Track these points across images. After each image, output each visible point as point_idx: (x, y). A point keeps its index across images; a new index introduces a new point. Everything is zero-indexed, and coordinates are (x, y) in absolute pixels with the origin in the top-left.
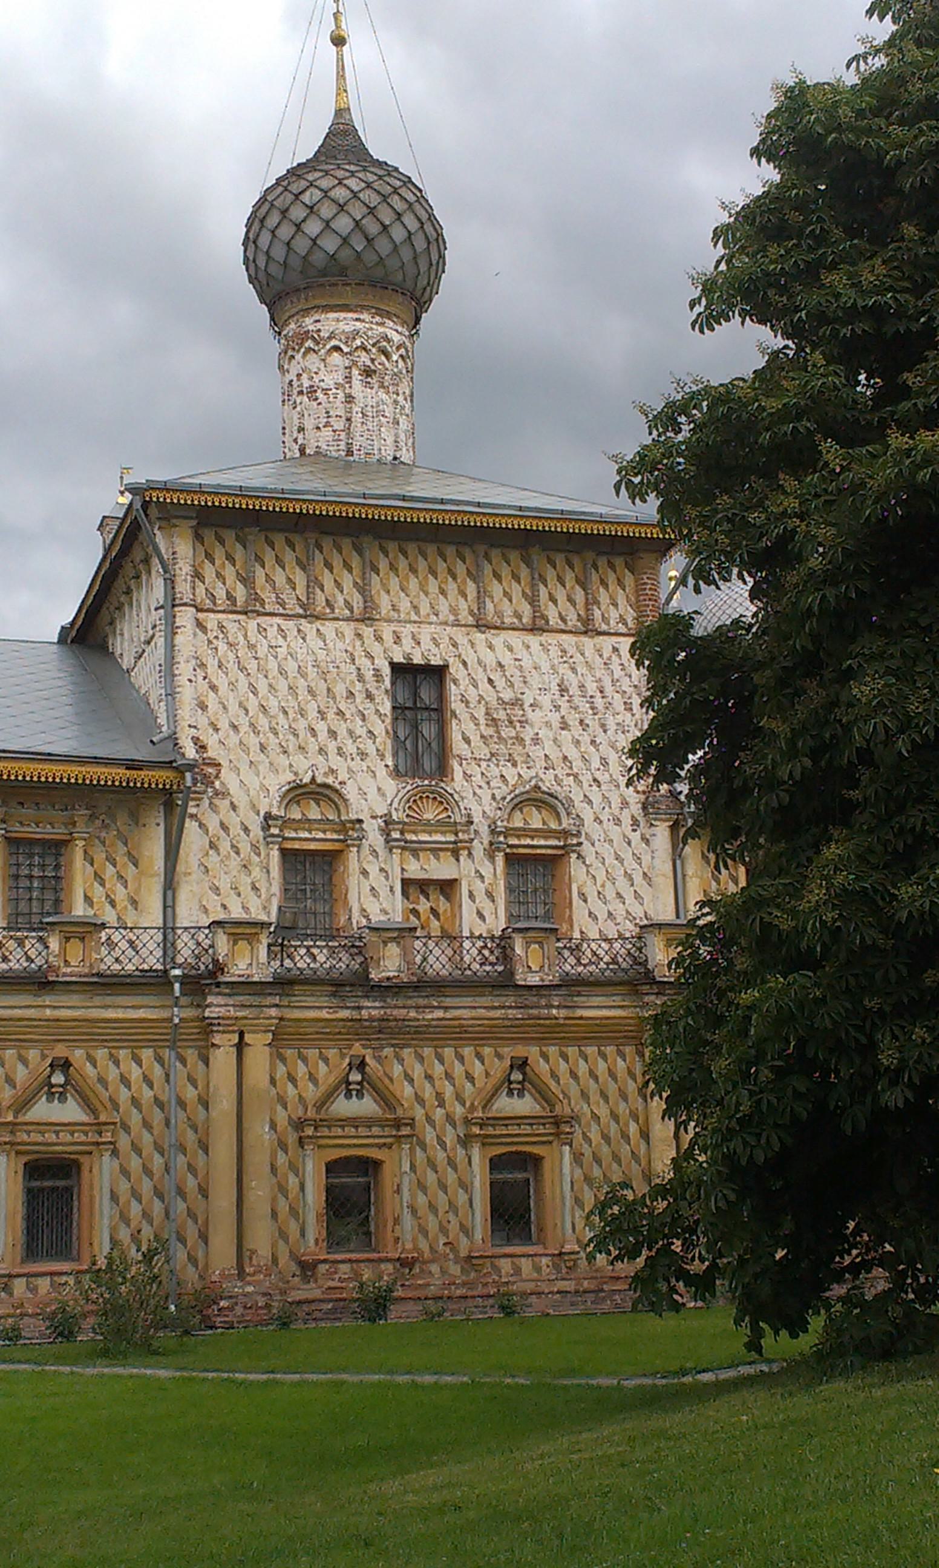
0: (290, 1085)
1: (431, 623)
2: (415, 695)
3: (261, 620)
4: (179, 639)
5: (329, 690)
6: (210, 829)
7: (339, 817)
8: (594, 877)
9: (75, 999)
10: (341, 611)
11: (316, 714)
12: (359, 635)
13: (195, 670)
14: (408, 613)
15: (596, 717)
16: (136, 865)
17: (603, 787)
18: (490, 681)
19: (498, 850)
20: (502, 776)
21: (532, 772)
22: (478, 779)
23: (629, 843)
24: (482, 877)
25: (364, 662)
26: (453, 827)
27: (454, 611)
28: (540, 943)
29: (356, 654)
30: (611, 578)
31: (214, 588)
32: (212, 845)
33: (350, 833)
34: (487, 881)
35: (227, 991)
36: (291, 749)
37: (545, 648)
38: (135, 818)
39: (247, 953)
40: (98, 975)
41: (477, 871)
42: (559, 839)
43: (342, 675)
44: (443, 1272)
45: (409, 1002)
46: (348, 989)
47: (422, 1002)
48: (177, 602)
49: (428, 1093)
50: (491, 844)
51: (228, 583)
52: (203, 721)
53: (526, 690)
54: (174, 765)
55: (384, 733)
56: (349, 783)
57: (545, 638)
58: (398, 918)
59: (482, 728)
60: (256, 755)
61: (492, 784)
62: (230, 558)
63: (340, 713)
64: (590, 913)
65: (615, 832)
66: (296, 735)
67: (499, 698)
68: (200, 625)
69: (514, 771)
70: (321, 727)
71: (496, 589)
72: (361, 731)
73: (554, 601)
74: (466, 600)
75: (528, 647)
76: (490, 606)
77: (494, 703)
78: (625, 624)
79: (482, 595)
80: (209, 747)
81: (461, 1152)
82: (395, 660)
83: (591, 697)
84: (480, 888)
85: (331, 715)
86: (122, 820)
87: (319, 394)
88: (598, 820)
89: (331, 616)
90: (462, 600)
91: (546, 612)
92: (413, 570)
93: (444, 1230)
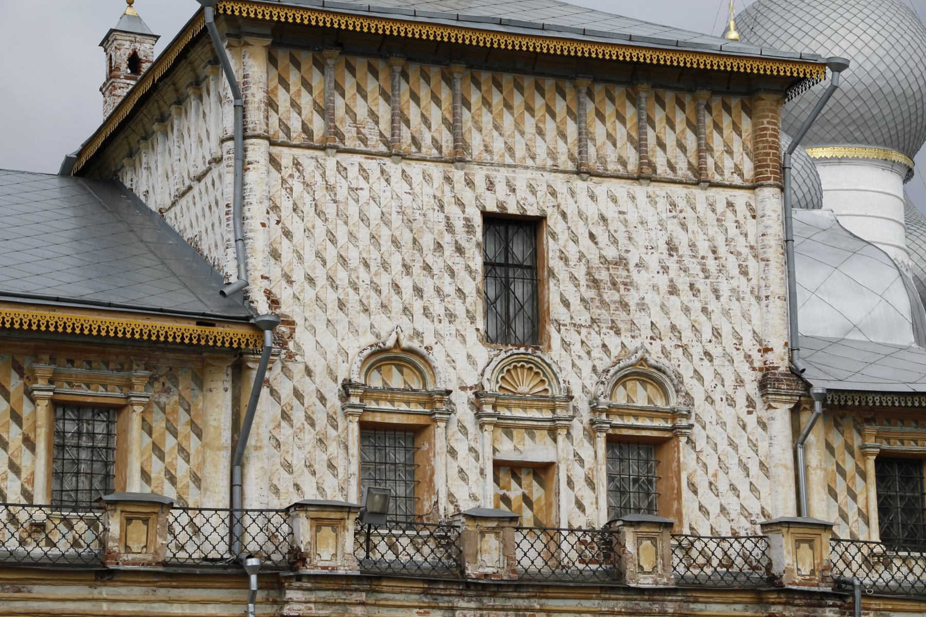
1: (527, 168)
2: (507, 250)
3: (341, 157)
4: (251, 177)
5: (415, 241)
6: (283, 397)
7: (424, 385)
8: (705, 465)
9: (136, 591)
10: (428, 150)
13: (268, 213)
14: (502, 156)
15: (708, 281)
16: (199, 436)
17: (716, 362)
18: (592, 236)
19: (600, 430)
20: (604, 346)
21: (637, 343)
22: (577, 348)
23: (744, 427)
24: (581, 461)
25: (453, 211)
26: (551, 403)
27: (552, 154)
28: (653, 540)
29: (445, 200)
30: (726, 121)
31: (289, 119)
32: (285, 416)
33: (438, 405)
34: (587, 466)
35: (309, 585)
38: (199, 381)
39: (331, 541)
40: (165, 564)
41: (576, 454)
42: (666, 419)
43: (430, 225)
45: (510, 603)
46: (441, 586)
47: (521, 603)
48: (249, 133)
50: (592, 422)
51: (304, 112)
52: (275, 272)
53: (631, 248)
54: (252, 321)
55: (474, 291)
56: (436, 348)
57: (654, 188)
58: (488, 504)
59: (583, 289)
60: (334, 313)
61: (593, 354)
63: (427, 268)
64: (701, 507)
65: (729, 415)
66: (378, 291)
67: (601, 257)
68: (274, 161)
70: (406, 284)
71: (599, 130)
72: (449, 289)
73: (662, 145)
74: (566, 142)
75: (633, 198)
76: (592, 150)
77: (595, 262)
78: (741, 175)
79: (584, 137)
80: (282, 301)
83: (703, 258)
84: (579, 474)
85: (417, 269)
86: (185, 382)
88: (709, 399)
89: (418, 155)
90: (561, 142)
91: (653, 160)
92: (508, 106)
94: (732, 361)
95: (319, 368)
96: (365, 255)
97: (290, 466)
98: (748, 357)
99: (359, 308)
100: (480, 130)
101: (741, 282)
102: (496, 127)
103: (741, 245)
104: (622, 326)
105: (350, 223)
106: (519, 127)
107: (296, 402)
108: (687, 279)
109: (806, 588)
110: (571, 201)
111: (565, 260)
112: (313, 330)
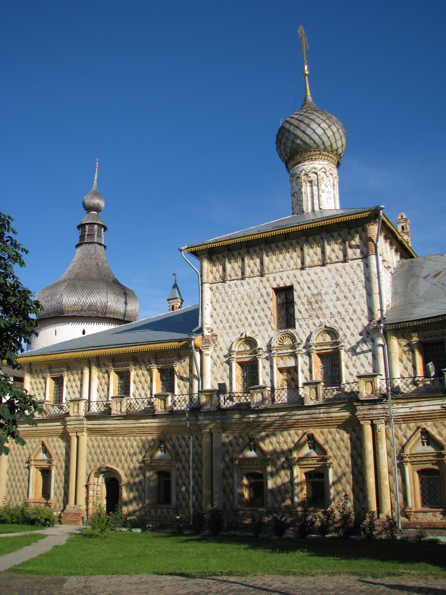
0: (230, 447)
5: (251, 303)
11: (247, 312)
17: (354, 321)
18: (309, 288)
20: (314, 323)
22: (304, 326)
36: (239, 327)
37: (330, 270)
43: (256, 296)
53: (322, 288)
60: (229, 330)
63: (256, 310)
66: (241, 321)
67: (312, 294)
68: (211, 289)
69: (318, 321)
70: (249, 317)
72: (262, 315)
77: (310, 296)
82: (274, 287)
83: (349, 286)
85: (252, 311)
87: (295, 195)
94: (360, 320)
96: (237, 311)
97: (216, 378)
99: (235, 327)
102: (277, 260)
104: (320, 316)
105: (232, 301)
107: (218, 359)
109: (368, 399)
110: (301, 278)
111: (299, 297)
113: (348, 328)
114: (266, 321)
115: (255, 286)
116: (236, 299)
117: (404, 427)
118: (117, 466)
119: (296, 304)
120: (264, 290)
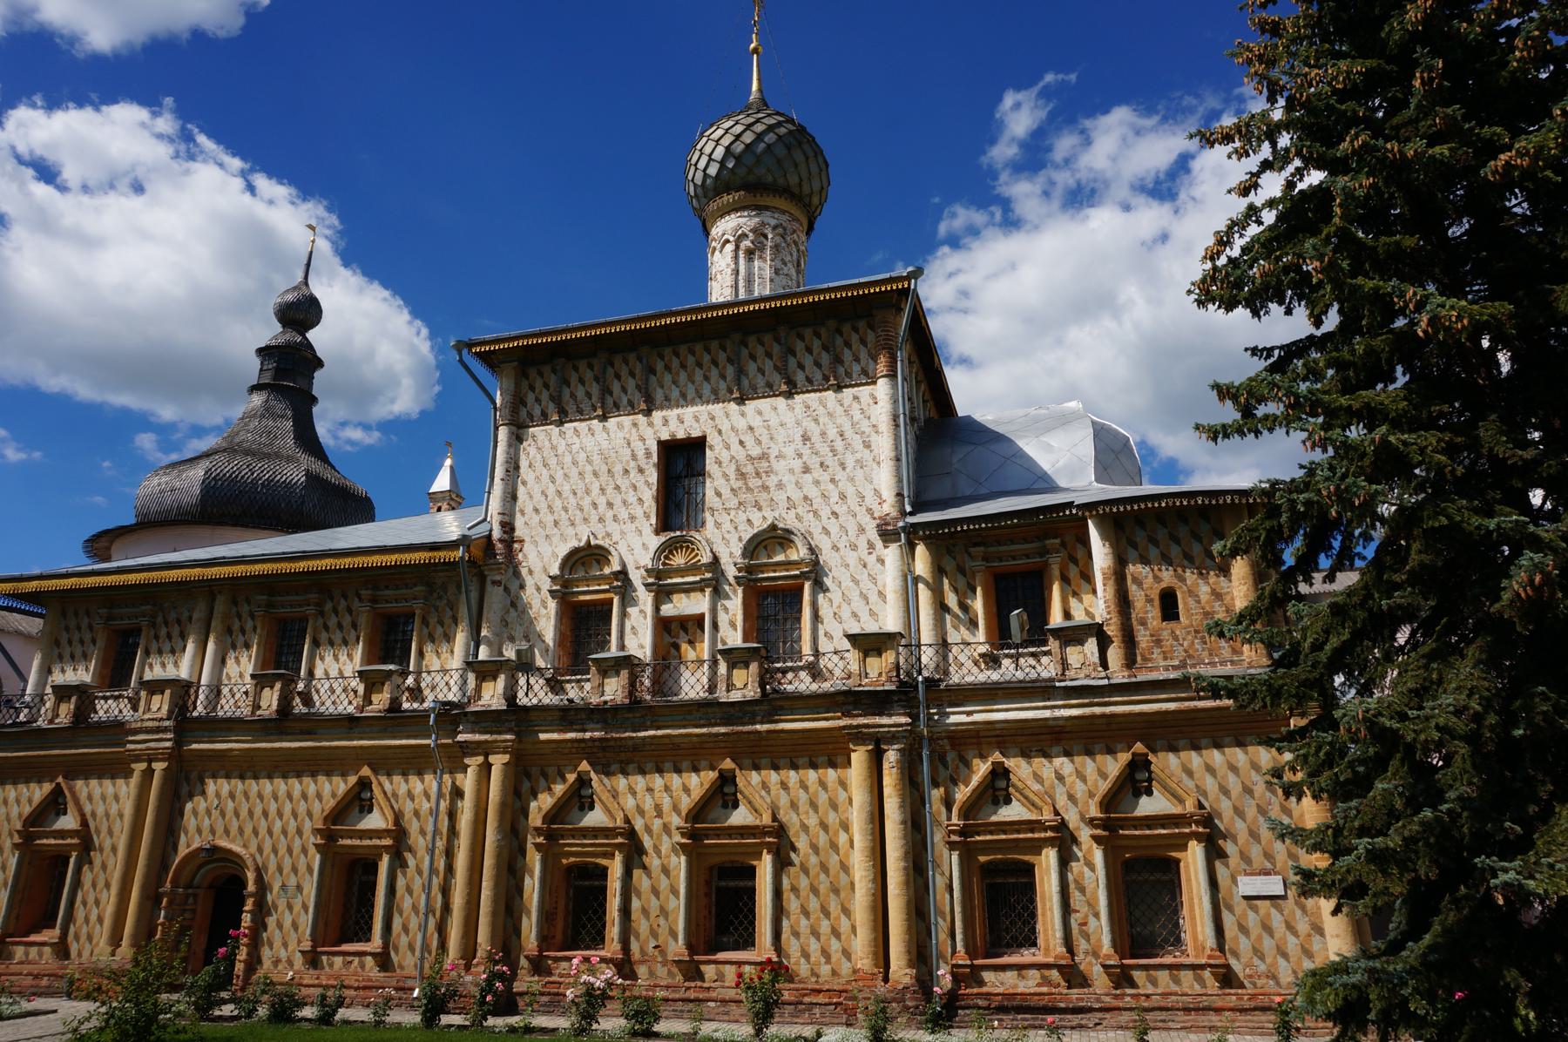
5: (609, 471)
12: (635, 425)
18: (741, 443)
22: (727, 526)
23: (865, 566)
30: (855, 338)
34: (731, 613)
36: (577, 522)
44: (652, 973)
49: (648, 804)
53: (772, 445)
62: (546, 386)
63: (617, 488)
65: (852, 557)
66: (582, 510)
69: (759, 515)
70: (602, 501)
72: (632, 498)
73: (801, 367)
81: (674, 859)
85: (610, 490)
92: (683, 366)
93: (654, 934)
95: (537, 569)
98: (869, 510)
99: (567, 523)
100: (662, 387)
101: (866, 454)
103: (865, 426)
106: (691, 379)
108: (819, 460)
110: (726, 421)
111: (719, 463)
112: (536, 543)
113: (826, 532)
114: (639, 512)
115: (620, 435)
116: (575, 463)
117: (953, 760)
118: (245, 846)
119: (710, 476)
120: (640, 443)
